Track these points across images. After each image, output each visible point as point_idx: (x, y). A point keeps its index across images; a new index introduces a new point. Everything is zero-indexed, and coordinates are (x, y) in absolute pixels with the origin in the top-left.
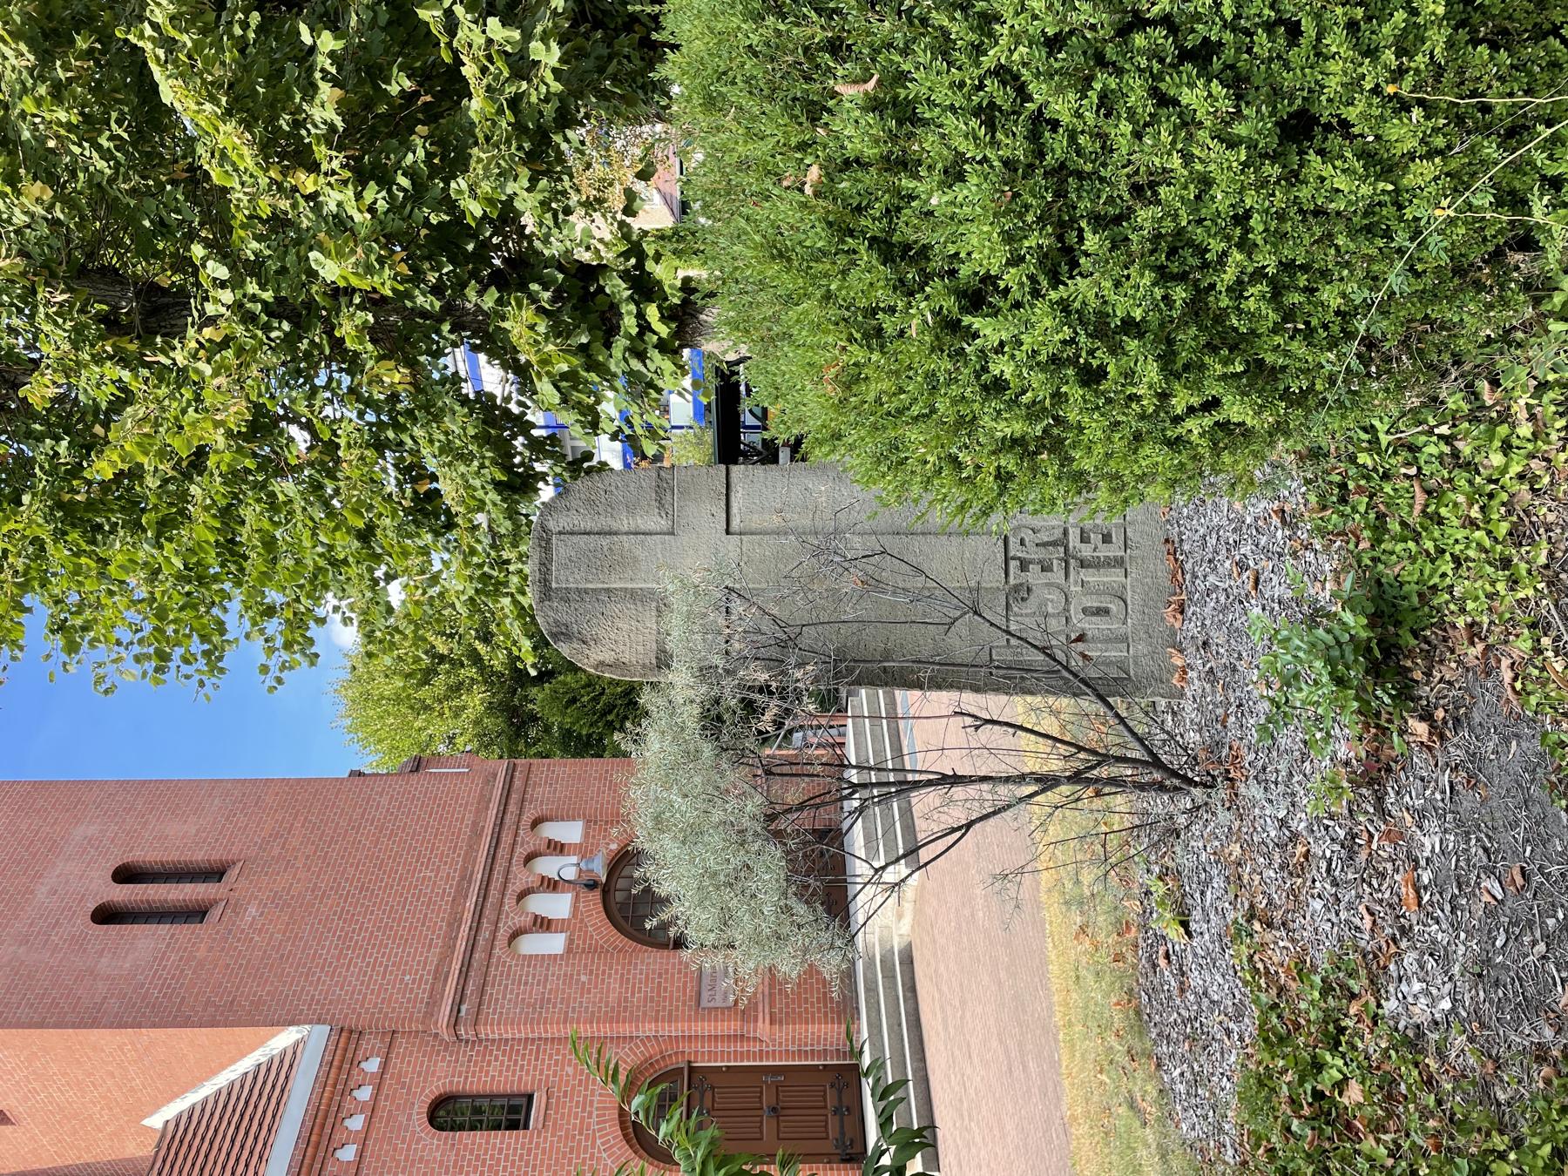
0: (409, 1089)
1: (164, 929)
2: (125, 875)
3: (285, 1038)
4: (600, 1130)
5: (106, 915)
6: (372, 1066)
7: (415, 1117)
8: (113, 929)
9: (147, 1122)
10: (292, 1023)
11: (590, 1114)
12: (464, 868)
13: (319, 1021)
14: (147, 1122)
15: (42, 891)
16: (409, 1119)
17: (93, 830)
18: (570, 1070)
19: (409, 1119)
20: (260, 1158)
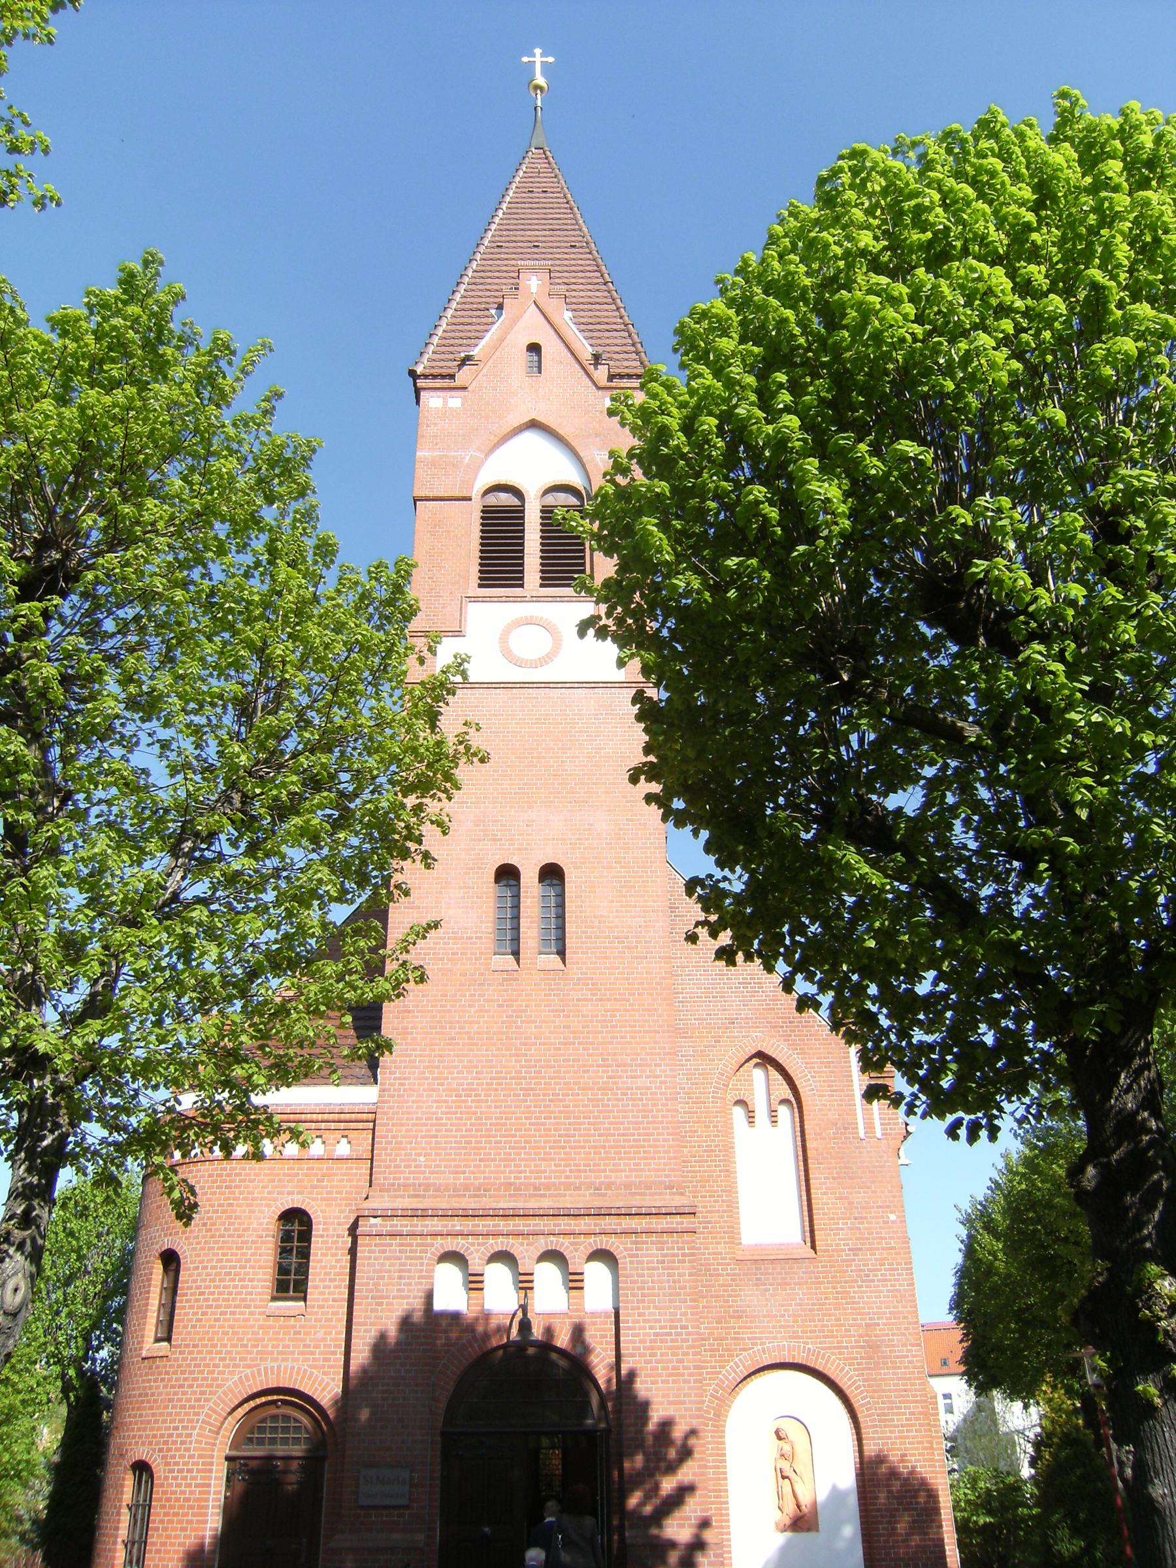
4: (259, 1371)
6: (343, 1149)
11: (273, 1360)
12: (547, 1187)
16: (289, 1193)
18: (320, 1335)
19: (289, 1193)
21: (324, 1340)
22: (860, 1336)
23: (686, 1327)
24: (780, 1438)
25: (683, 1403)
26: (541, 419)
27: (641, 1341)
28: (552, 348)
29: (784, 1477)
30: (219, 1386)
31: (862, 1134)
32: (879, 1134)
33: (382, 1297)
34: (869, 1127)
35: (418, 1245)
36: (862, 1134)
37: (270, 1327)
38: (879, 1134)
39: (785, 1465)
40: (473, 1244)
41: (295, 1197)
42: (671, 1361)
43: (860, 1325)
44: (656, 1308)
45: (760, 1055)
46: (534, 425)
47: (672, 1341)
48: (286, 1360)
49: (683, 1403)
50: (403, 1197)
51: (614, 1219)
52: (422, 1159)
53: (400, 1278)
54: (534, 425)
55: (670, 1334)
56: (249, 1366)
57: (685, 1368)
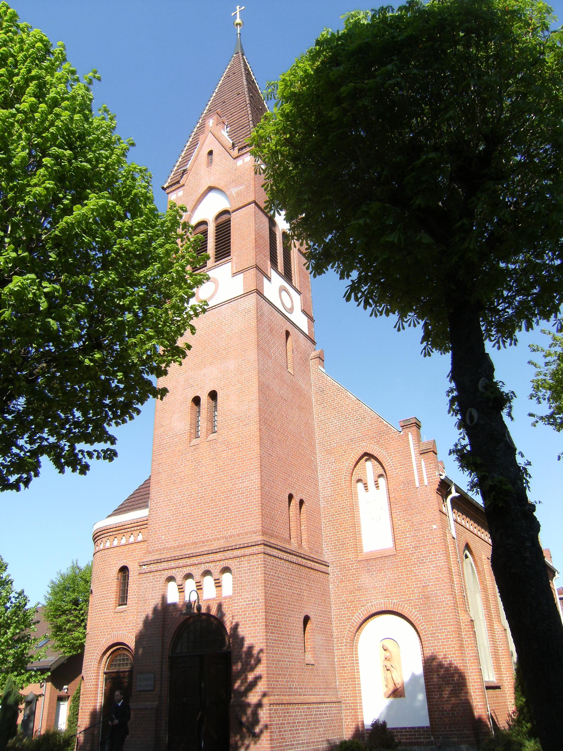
11: (116, 631)
18: (131, 619)
21: (132, 621)
22: (419, 593)
23: (258, 600)
24: (385, 650)
25: (257, 636)
26: (212, 185)
27: (241, 609)
28: (217, 149)
29: (388, 670)
30: (100, 644)
31: (417, 485)
32: (426, 483)
33: (146, 600)
34: (421, 480)
35: (159, 575)
36: (417, 485)
37: (116, 617)
38: (426, 483)
39: (388, 664)
40: (178, 572)
41: (124, 561)
42: (252, 617)
43: (419, 587)
44: (247, 592)
45: (366, 454)
46: (211, 189)
47: (253, 607)
48: (120, 630)
49: (257, 636)
50: (156, 555)
51: (231, 552)
52: (163, 537)
53: (153, 590)
55: (252, 604)
56: (108, 635)
57: (258, 620)
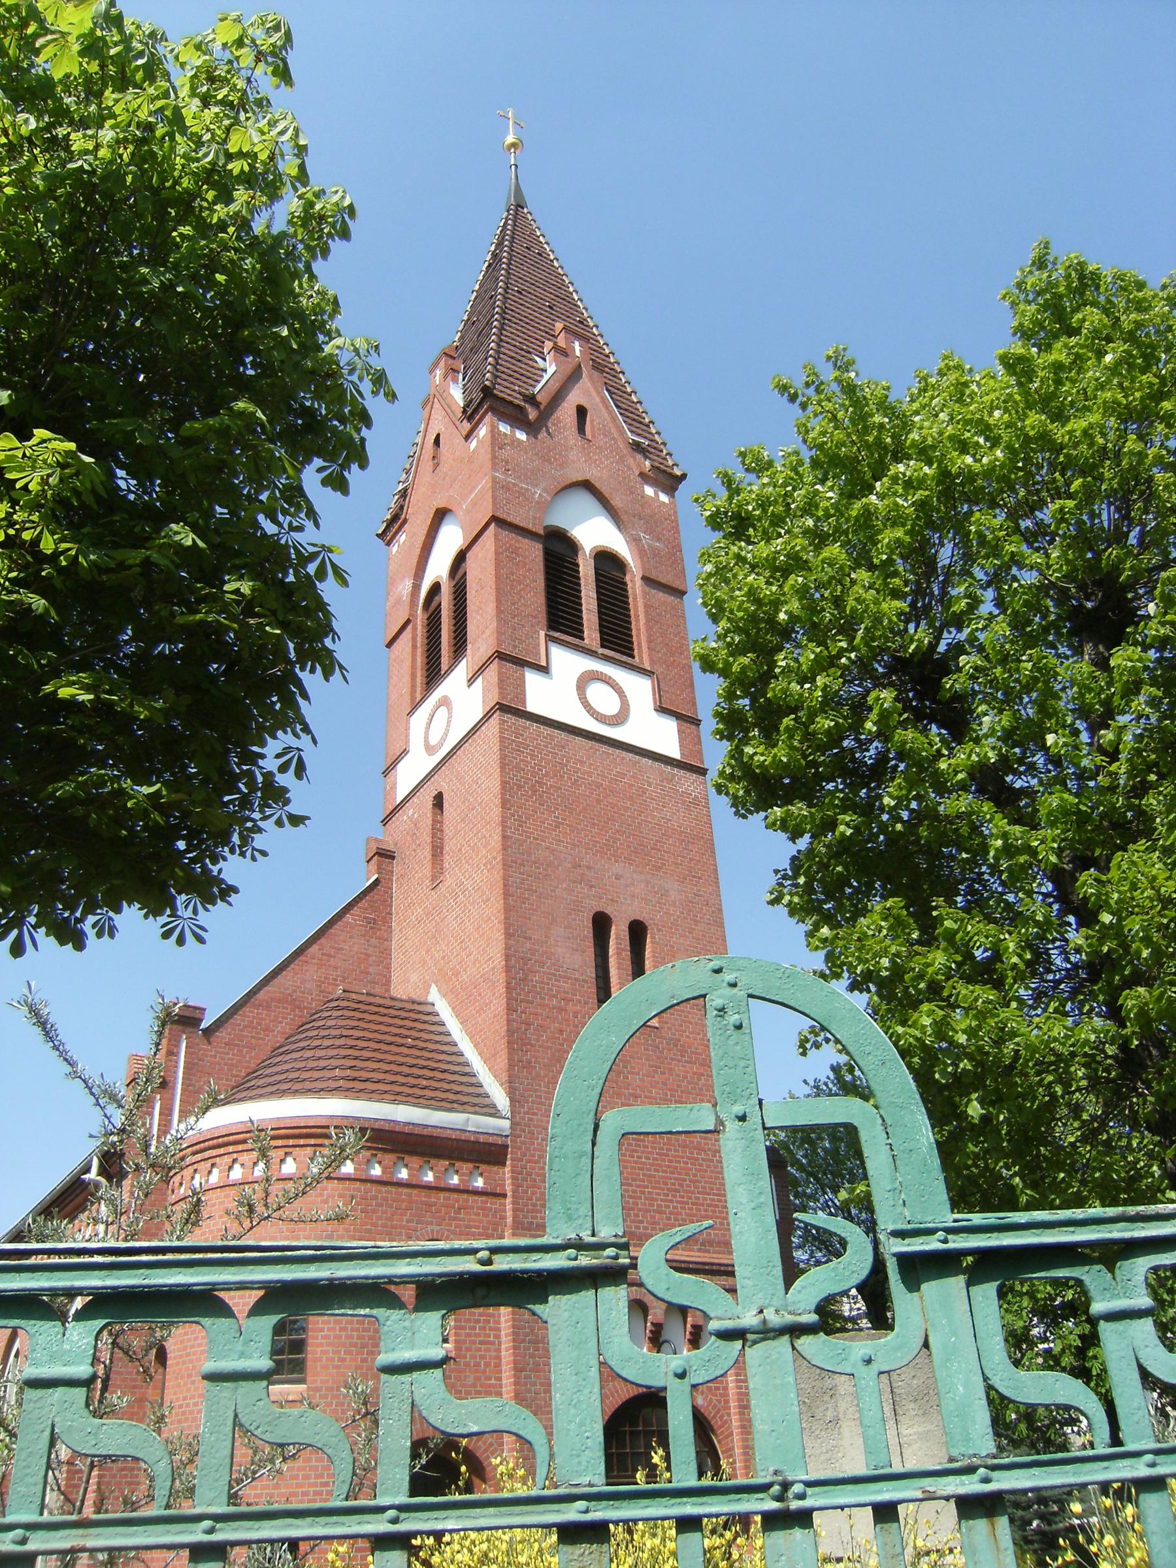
0: (455, 1219)
1: (591, 972)
2: (637, 931)
3: (501, 1099)
5: (601, 924)
7: (429, 1228)
8: (588, 931)
9: (434, 989)
10: (513, 1101)
13: (514, 1125)
14: (434, 989)
15: (617, 868)
17: (674, 895)
20: (398, 1093)
46: (587, 485)
54: (587, 485)
